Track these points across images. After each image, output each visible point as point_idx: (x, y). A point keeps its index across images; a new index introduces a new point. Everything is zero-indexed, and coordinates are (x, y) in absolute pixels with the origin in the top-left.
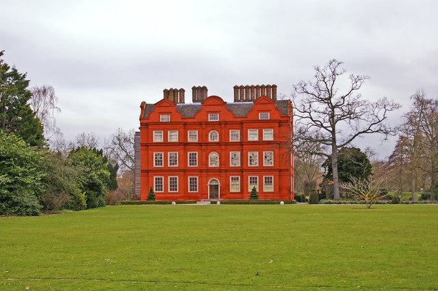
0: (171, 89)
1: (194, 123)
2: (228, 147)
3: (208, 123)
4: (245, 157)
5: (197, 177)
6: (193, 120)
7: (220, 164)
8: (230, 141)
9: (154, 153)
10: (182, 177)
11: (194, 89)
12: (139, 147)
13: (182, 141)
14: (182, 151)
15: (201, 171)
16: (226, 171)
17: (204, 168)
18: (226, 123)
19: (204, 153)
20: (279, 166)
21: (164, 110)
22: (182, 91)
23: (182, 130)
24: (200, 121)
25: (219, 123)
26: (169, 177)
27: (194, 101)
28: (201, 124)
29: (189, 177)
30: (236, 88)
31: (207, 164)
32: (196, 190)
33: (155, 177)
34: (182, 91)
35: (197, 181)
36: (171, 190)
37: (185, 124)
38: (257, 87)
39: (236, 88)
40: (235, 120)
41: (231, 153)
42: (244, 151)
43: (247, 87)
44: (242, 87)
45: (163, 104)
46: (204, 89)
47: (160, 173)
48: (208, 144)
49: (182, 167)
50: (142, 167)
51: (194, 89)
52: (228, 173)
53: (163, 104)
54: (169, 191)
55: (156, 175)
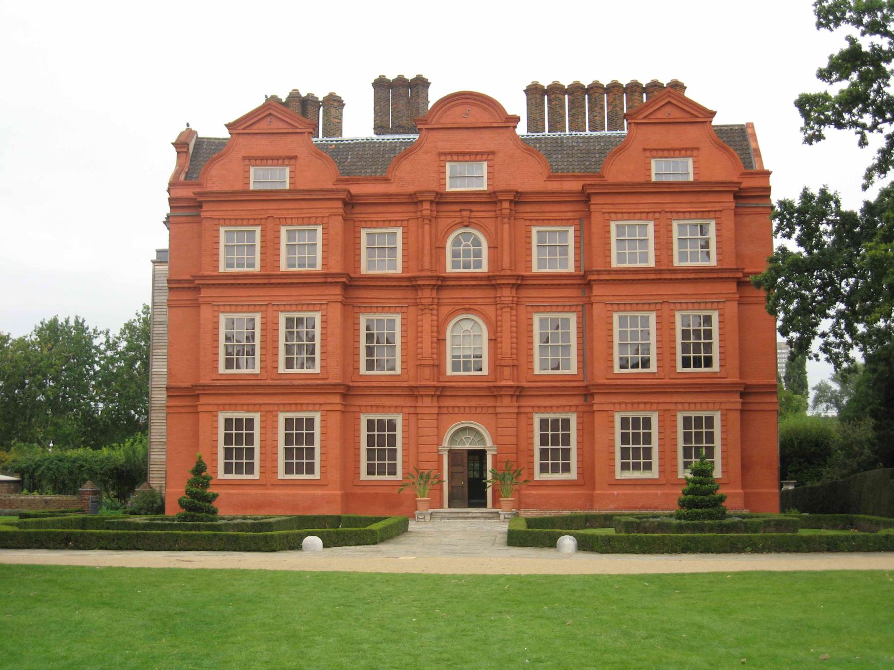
0: (294, 96)
1: (388, 201)
2: (524, 293)
3: (440, 200)
4: (598, 333)
5: (399, 420)
6: (380, 188)
7: (496, 365)
8: (535, 270)
9: (223, 318)
10: (335, 419)
11: (380, 85)
12: (164, 296)
13: (336, 269)
14: (336, 311)
15: (413, 392)
16: (519, 392)
17: (426, 378)
18: (518, 199)
19: (427, 322)
20: (742, 375)
21: (262, 146)
22: (334, 103)
23: (337, 224)
24: (411, 189)
25: (491, 199)
26: (281, 418)
27: (380, 128)
28: (414, 200)
29: (363, 420)
30: (534, 92)
31: (438, 366)
32: (393, 472)
33: (222, 417)
34: (334, 103)
35: (399, 433)
36: (288, 470)
37: (350, 203)
38: (615, 88)
39: (534, 92)
40: (554, 186)
41: (537, 318)
42: (597, 309)
43: (576, 90)
44: (555, 90)
45: (263, 126)
46: (421, 84)
47: (245, 400)
48: (442, 283)
49: (335, 377)
50: (170, 374)
51: (380, 85)
52: (524, 402)
53: (263, 126)
54: (281, 475)
55: (225, 407)
